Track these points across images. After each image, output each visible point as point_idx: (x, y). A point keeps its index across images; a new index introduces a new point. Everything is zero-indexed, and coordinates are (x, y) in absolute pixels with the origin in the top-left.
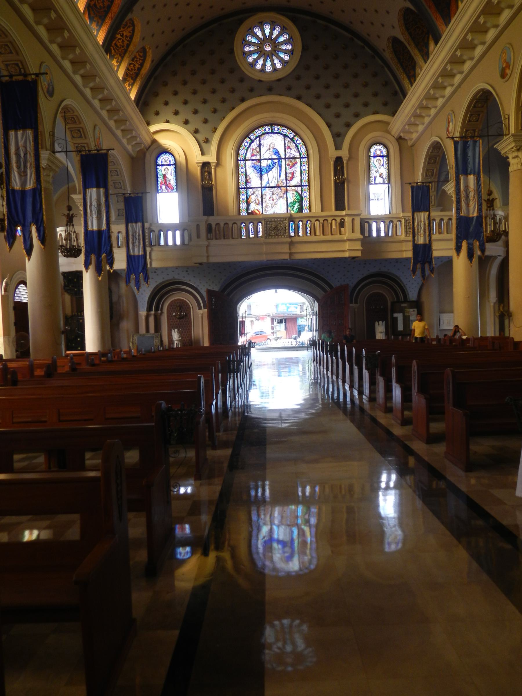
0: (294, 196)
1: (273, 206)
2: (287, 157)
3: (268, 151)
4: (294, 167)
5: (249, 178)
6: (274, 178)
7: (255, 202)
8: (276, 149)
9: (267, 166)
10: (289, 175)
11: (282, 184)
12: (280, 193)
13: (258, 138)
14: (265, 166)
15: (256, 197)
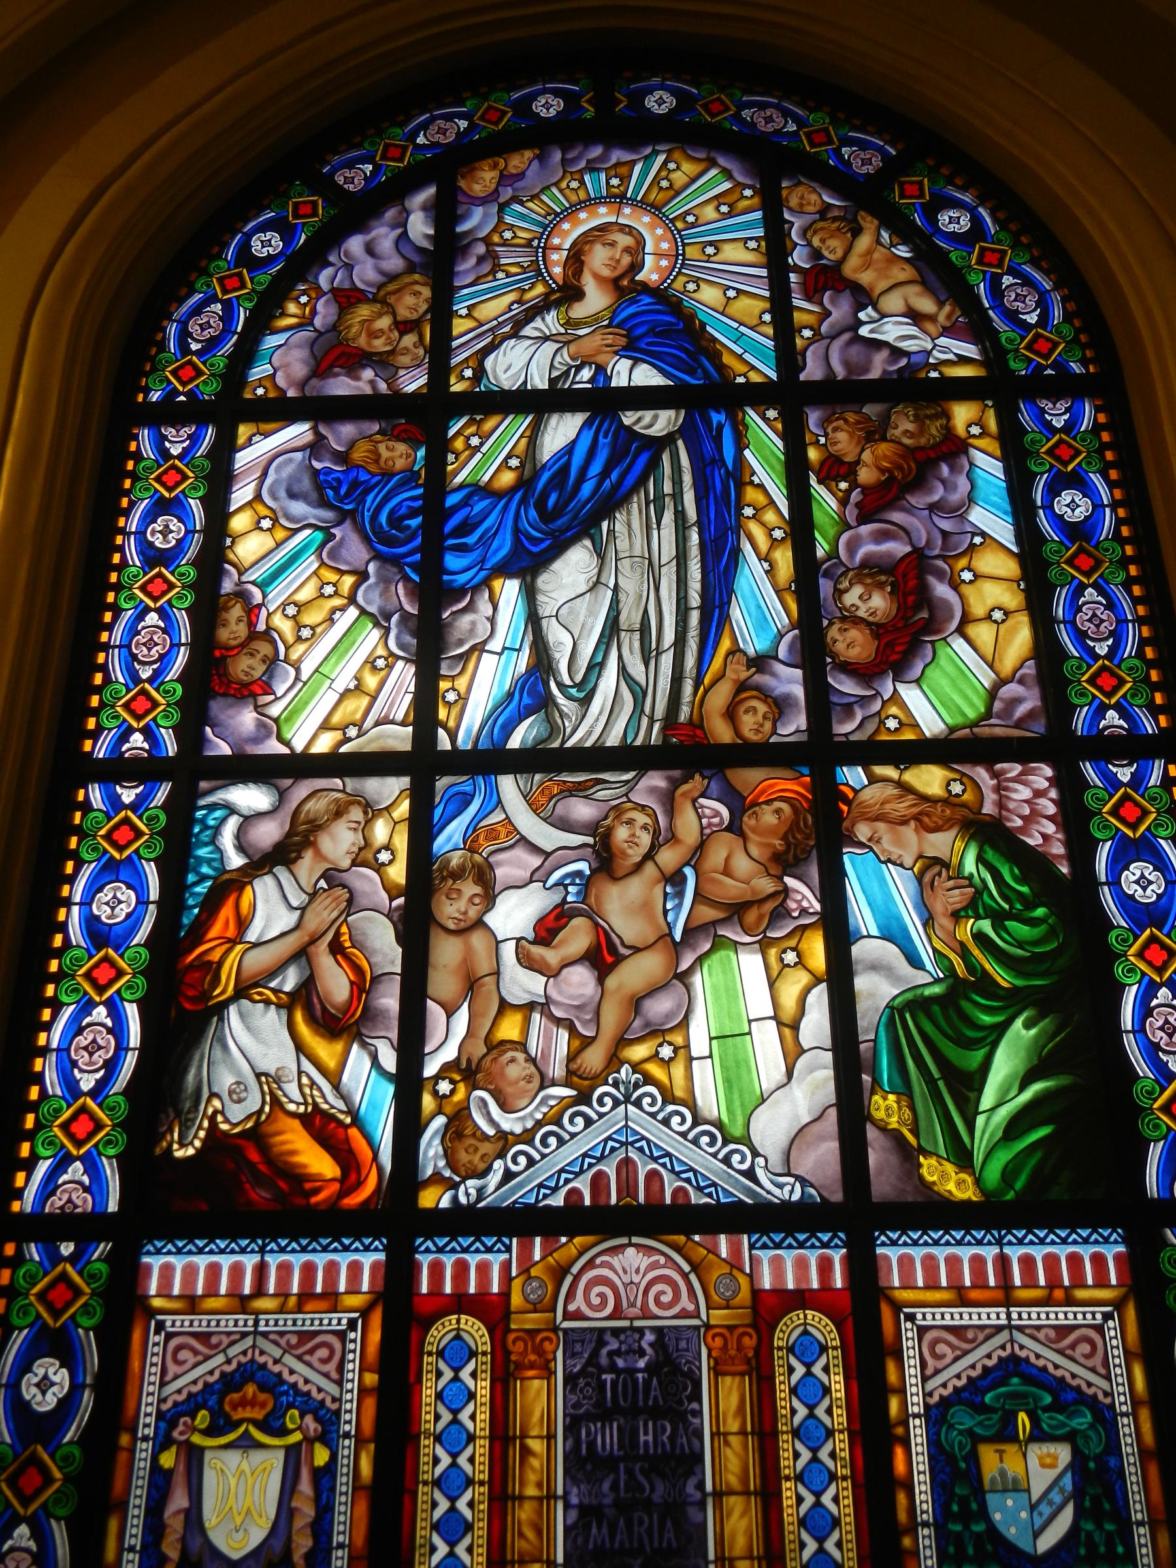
0: (957, 898)
1: (594, 1058)
2: (812, 371)
3: (551, 322)
4: (918, 500)
5: (253, 635)
6: (631, 644)
7: (290, 980)
8: (658, 293)
9: (524, 484)
10: (852, 597)
11: (748, 723)
12: (716, 856)
13: (431, 191)
14: (507, 479)
15: (324, 913)
